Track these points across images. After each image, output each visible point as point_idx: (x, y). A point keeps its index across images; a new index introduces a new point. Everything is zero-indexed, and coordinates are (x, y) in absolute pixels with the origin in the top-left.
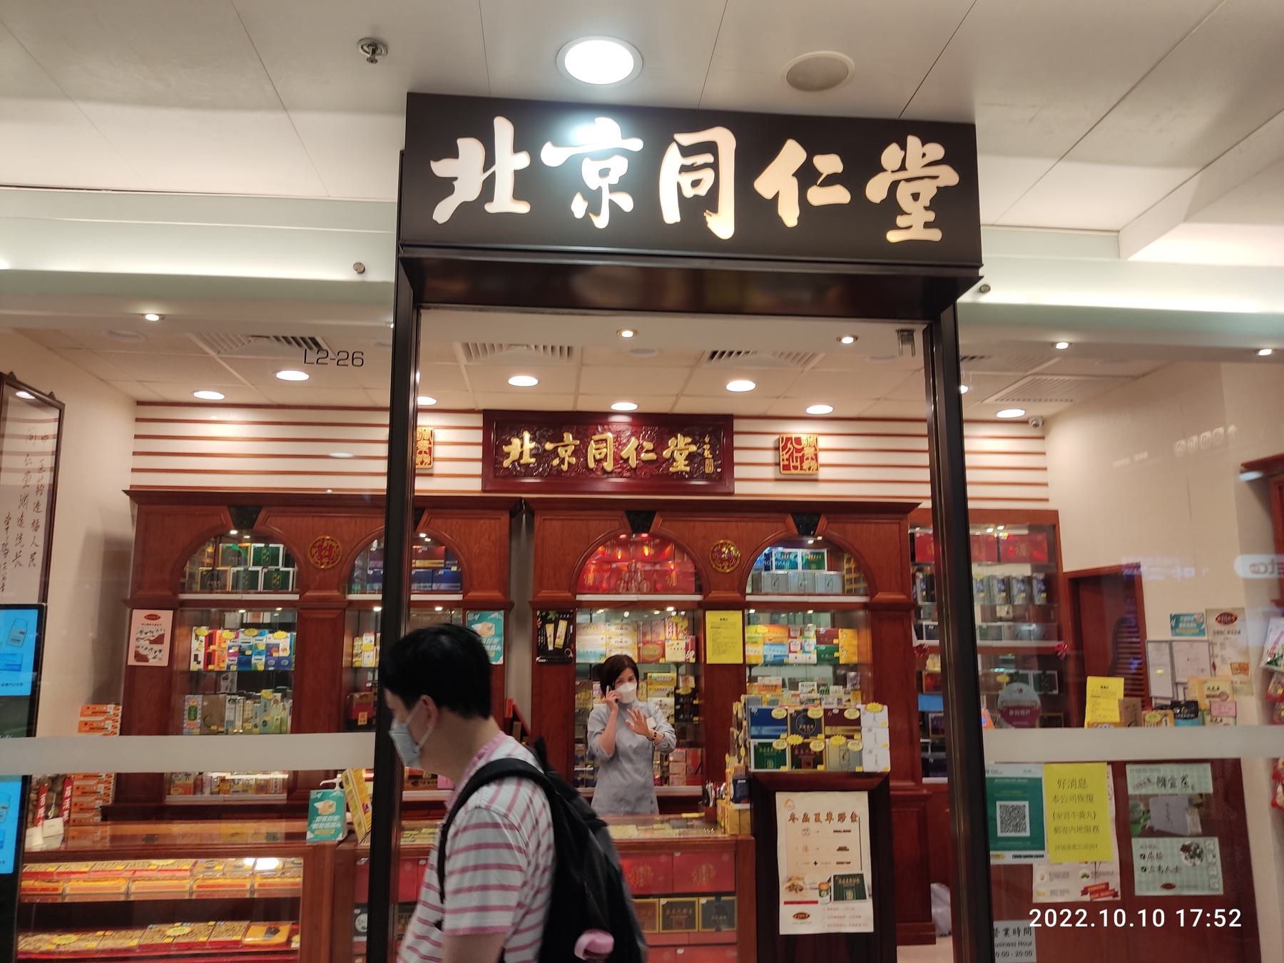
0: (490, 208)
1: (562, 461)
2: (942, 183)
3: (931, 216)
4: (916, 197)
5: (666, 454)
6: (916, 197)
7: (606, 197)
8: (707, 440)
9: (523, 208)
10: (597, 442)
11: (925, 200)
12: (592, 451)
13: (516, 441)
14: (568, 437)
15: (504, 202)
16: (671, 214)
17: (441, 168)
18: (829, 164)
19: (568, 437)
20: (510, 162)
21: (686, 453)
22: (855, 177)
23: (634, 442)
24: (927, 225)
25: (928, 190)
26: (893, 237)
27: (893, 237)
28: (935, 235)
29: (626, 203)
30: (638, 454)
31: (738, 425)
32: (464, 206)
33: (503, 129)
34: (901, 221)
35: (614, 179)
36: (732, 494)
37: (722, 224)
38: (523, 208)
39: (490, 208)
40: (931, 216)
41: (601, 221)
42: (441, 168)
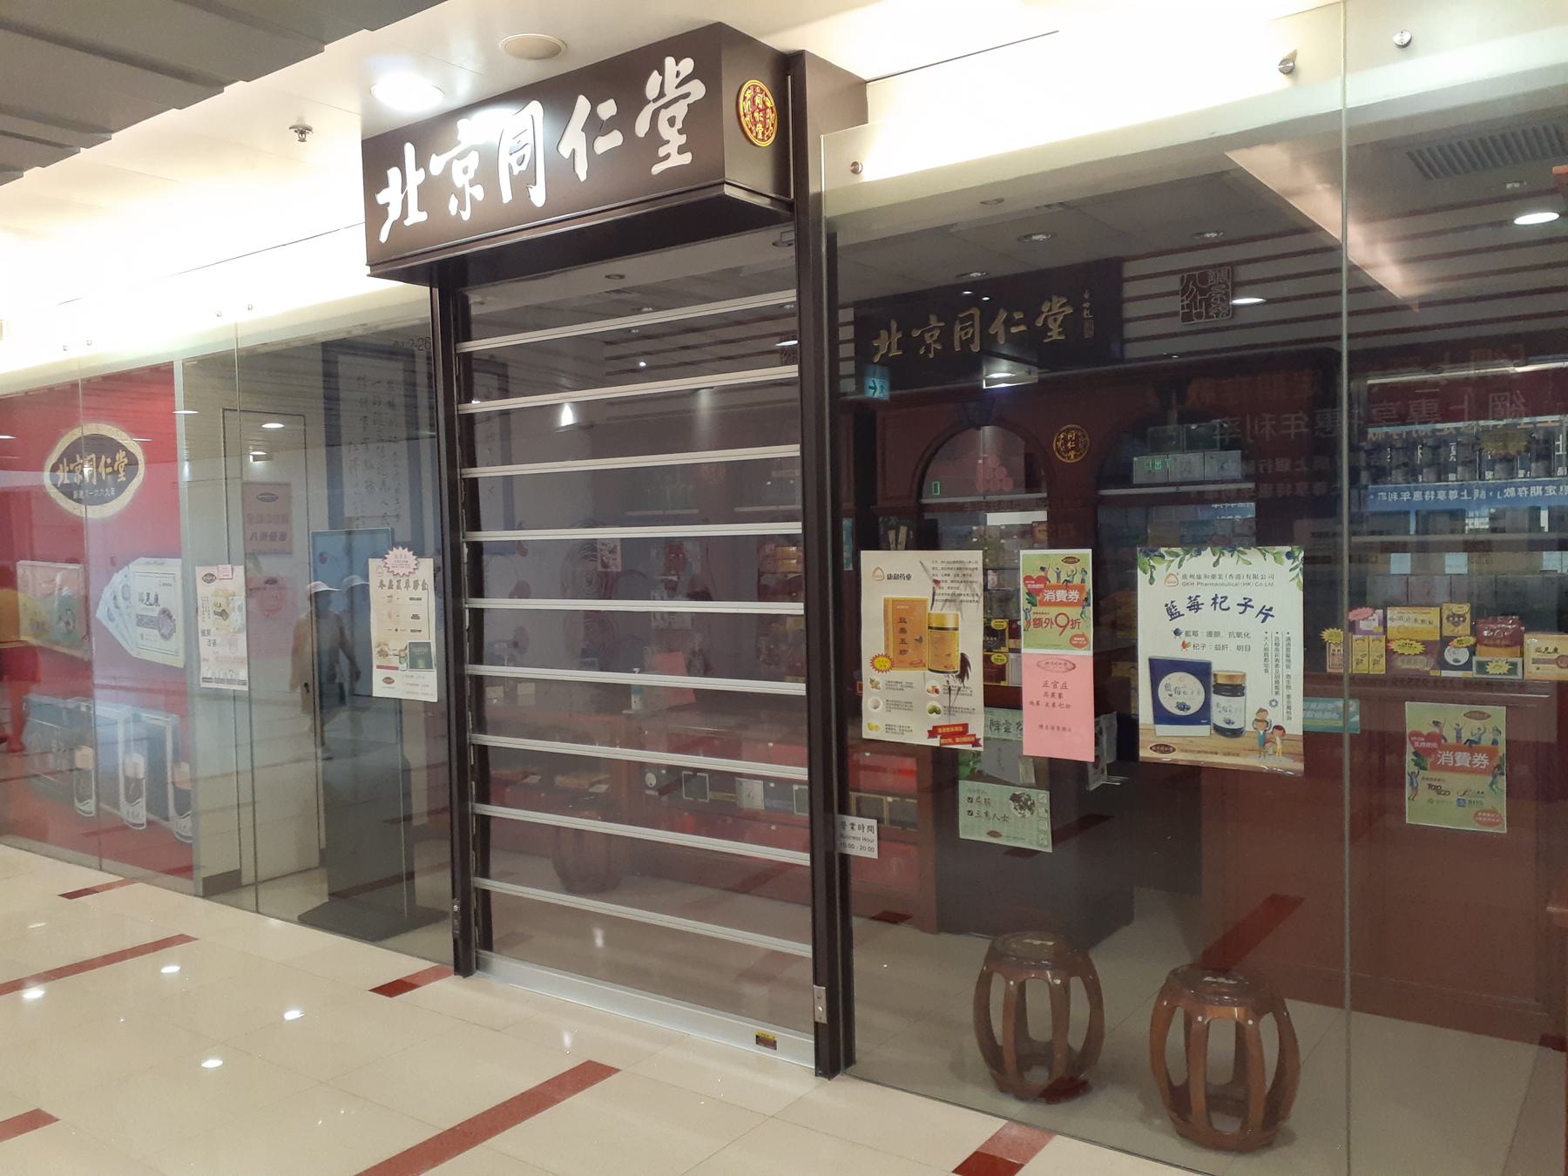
0: (407, 223)
1: (928, 350)
2: (690, 100)
3: (683, 139)
4: (672, 122)
5: (1039, 323)
6: (672, 122)
7: (468, 190)
8: (1086, 296)
9: (423, 217)
10: (963, 321)
11: (679, 125)
12: (958, 334)
13: (884, 333)
14: (933, 321)
15: (416, 217)
16: (507, 197)
17: (382, 198)
18: (608, 109)
19: (933, 321)
20: (415, 177)
21: (1060, 318)
22: (623, 121)
23: (1003, 315)
24: (681, 150)
25: (680, 110)
26: (657, 169)
27: (657, 169)
28: (687, 158)
29: (478, 192)
30: (1007, 332)
31: (1130, 269)
32: (397, 224)
33: (409, 150)
34: (662, 152)
35: (471, 175)
36: (1122, 360)
37: (538, 196)
38: (423, 217)
39: (407, 223)
40: (683, 139)
41: (466, 215)
42: (382, 198)
